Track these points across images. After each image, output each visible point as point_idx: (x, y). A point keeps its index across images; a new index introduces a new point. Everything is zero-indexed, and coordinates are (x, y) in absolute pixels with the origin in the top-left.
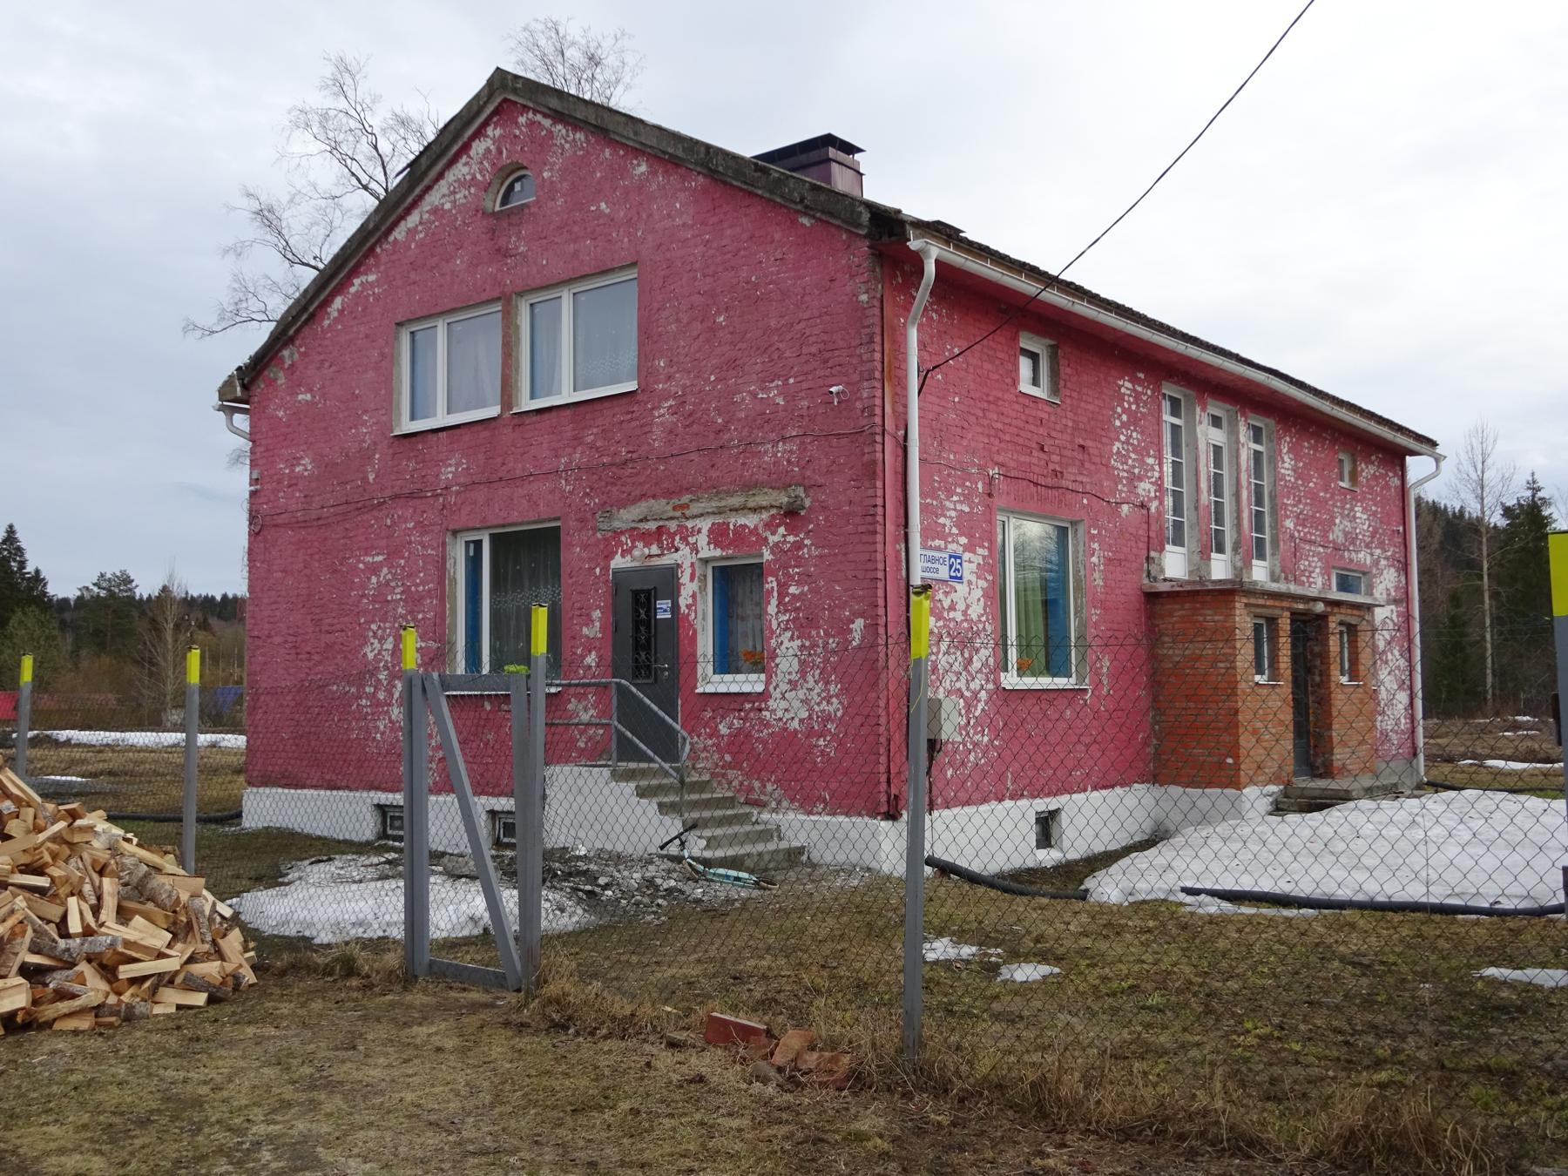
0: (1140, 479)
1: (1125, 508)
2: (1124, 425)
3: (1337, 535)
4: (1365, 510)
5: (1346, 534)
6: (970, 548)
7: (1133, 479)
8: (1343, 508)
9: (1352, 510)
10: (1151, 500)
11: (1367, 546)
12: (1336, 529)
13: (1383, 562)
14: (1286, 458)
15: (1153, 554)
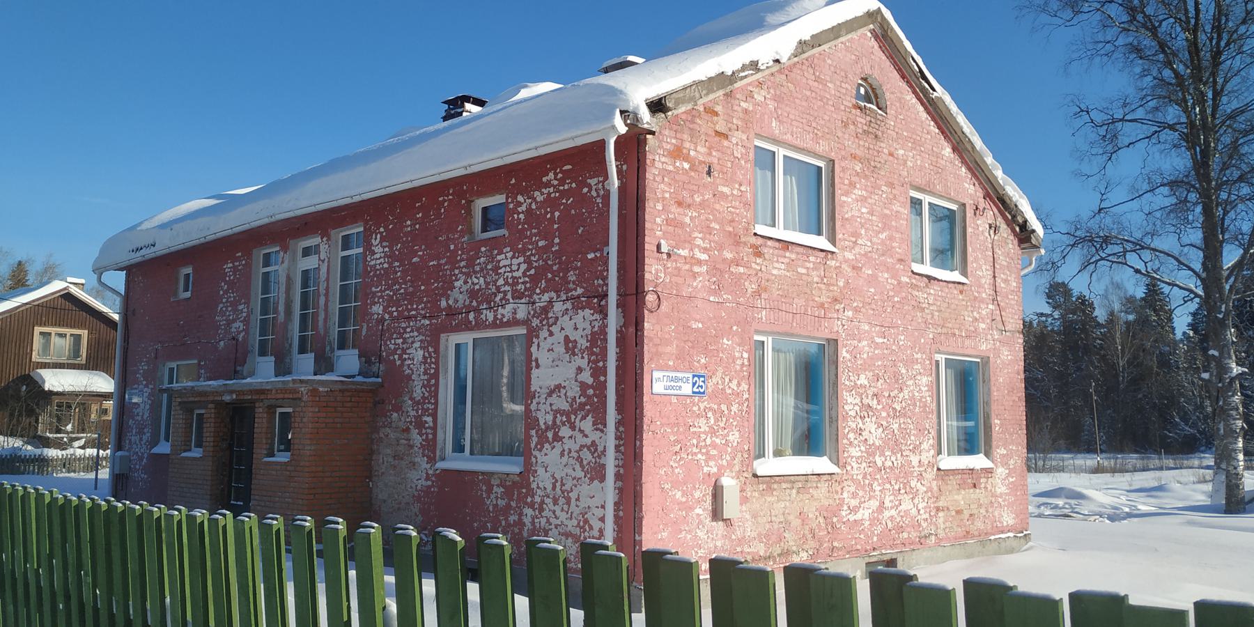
0: (234, 321)
1: (222, 343)
2: (226, 292)
3: (458, 296)
4: (517, 252)
5: (473, 294)
6: (146, 386)
7: (229, 323)
8: (471, 264)
9: (492, 258)
10: (239, 333)
11: (518, 295)
12: (455, 294)
13: (558, 307)
14: (378, 249)
15: (239, 368)
